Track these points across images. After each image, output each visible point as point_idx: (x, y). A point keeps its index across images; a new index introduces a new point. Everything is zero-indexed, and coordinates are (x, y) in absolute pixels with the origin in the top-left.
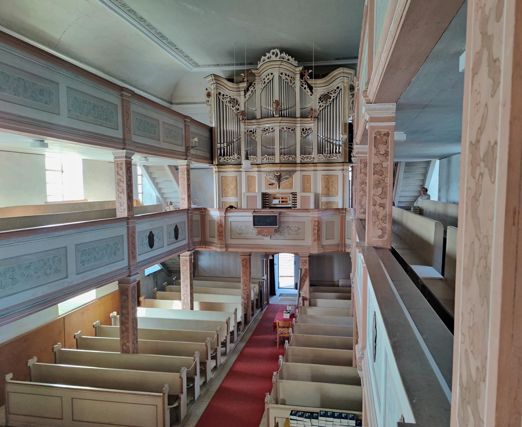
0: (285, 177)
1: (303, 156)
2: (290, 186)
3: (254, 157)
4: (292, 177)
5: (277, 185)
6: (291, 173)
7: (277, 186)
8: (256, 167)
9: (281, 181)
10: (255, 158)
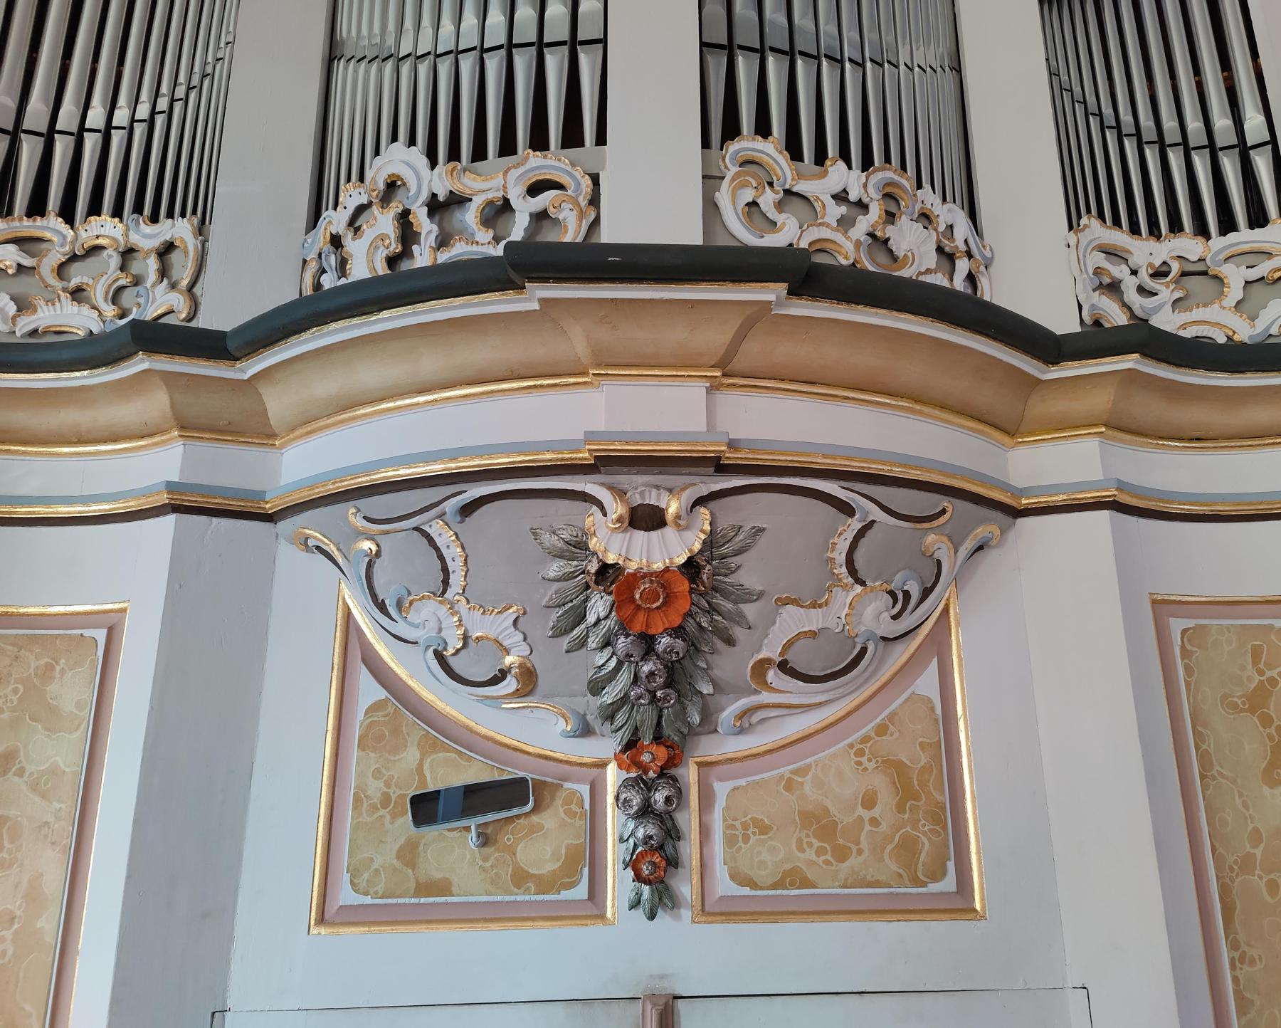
0: (813, 620)
1: (1120, 238)
2: (907, 849)
3: (147, 236)
4: (939, 643)
5: (614, 821)
6: (934, 541)
7: (613, 854)
8: (156, 404)
9: (708, 723)
10: (168, 249)
